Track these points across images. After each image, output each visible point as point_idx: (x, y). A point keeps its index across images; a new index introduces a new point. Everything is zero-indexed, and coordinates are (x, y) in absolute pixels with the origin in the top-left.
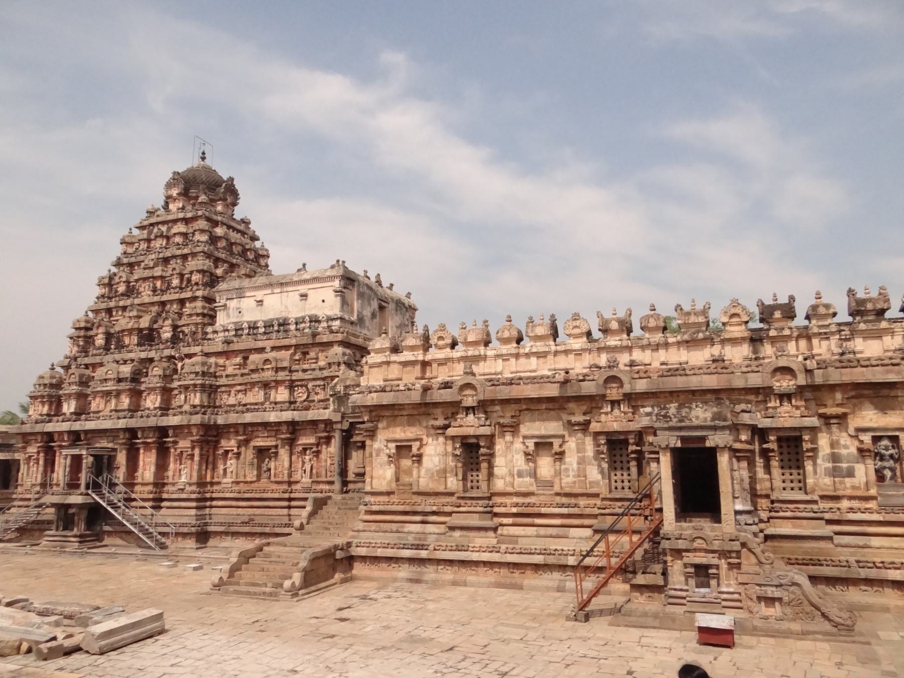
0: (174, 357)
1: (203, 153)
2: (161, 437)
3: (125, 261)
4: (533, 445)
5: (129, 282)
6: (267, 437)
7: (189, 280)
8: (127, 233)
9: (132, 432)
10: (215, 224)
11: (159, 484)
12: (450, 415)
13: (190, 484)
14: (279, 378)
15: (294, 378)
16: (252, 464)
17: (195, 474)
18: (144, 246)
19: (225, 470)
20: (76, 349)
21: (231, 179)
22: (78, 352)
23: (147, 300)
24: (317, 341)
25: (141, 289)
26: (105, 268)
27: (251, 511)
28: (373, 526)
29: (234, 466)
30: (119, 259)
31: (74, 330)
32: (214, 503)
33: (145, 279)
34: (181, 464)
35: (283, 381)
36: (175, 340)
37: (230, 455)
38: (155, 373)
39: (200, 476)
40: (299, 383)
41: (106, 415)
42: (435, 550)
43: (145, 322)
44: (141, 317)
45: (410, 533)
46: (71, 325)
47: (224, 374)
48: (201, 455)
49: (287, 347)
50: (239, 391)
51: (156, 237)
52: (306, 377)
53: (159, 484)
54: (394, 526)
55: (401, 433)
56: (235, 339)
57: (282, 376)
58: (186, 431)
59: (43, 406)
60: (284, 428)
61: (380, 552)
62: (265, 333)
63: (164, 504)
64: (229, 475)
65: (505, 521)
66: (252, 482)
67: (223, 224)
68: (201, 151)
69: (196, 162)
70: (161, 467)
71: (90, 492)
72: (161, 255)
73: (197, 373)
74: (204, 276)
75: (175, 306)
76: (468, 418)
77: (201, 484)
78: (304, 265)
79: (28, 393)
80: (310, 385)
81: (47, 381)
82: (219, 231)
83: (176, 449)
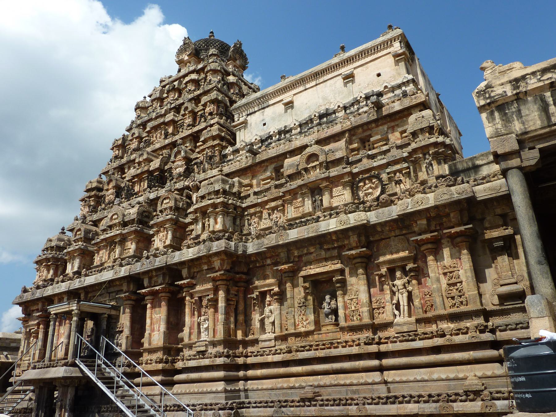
3: (139, 122)
9: (135, 280)
10: (228, 74)
11: (172, 348)
13: (214, 344)
15: (355, 171)
16: (304, 305)
17: (220, 328)
19: (262, 322)
22: (88, 212)
23: (158, 146)
24: (385, 113)
27: (312, 380)
29: (277, 312)
32: (250, 373)
34: (200, 315)
36: (188, 173)
37: (268, 298)
38: (164, 206)
39: (227, 331)
41: (110, 268)
43: (156, 164)
47: (251, 192)
48: (227, 300)
49: (335, 137)
50: (273, 209)
51: (168, 93)
52: (375, 164)
53: (172, 348)
58: (206, 267)
59: (48, 271)
63: (177, 377)
64: (268, 328)
66: (308, 334)
70: (175, 324)
71: (77, 362)
73: (217, 192)
74: (218, 107)
77: (229, 342)
80: (384, 176)
81: (53, 244)
83: (192, 296)
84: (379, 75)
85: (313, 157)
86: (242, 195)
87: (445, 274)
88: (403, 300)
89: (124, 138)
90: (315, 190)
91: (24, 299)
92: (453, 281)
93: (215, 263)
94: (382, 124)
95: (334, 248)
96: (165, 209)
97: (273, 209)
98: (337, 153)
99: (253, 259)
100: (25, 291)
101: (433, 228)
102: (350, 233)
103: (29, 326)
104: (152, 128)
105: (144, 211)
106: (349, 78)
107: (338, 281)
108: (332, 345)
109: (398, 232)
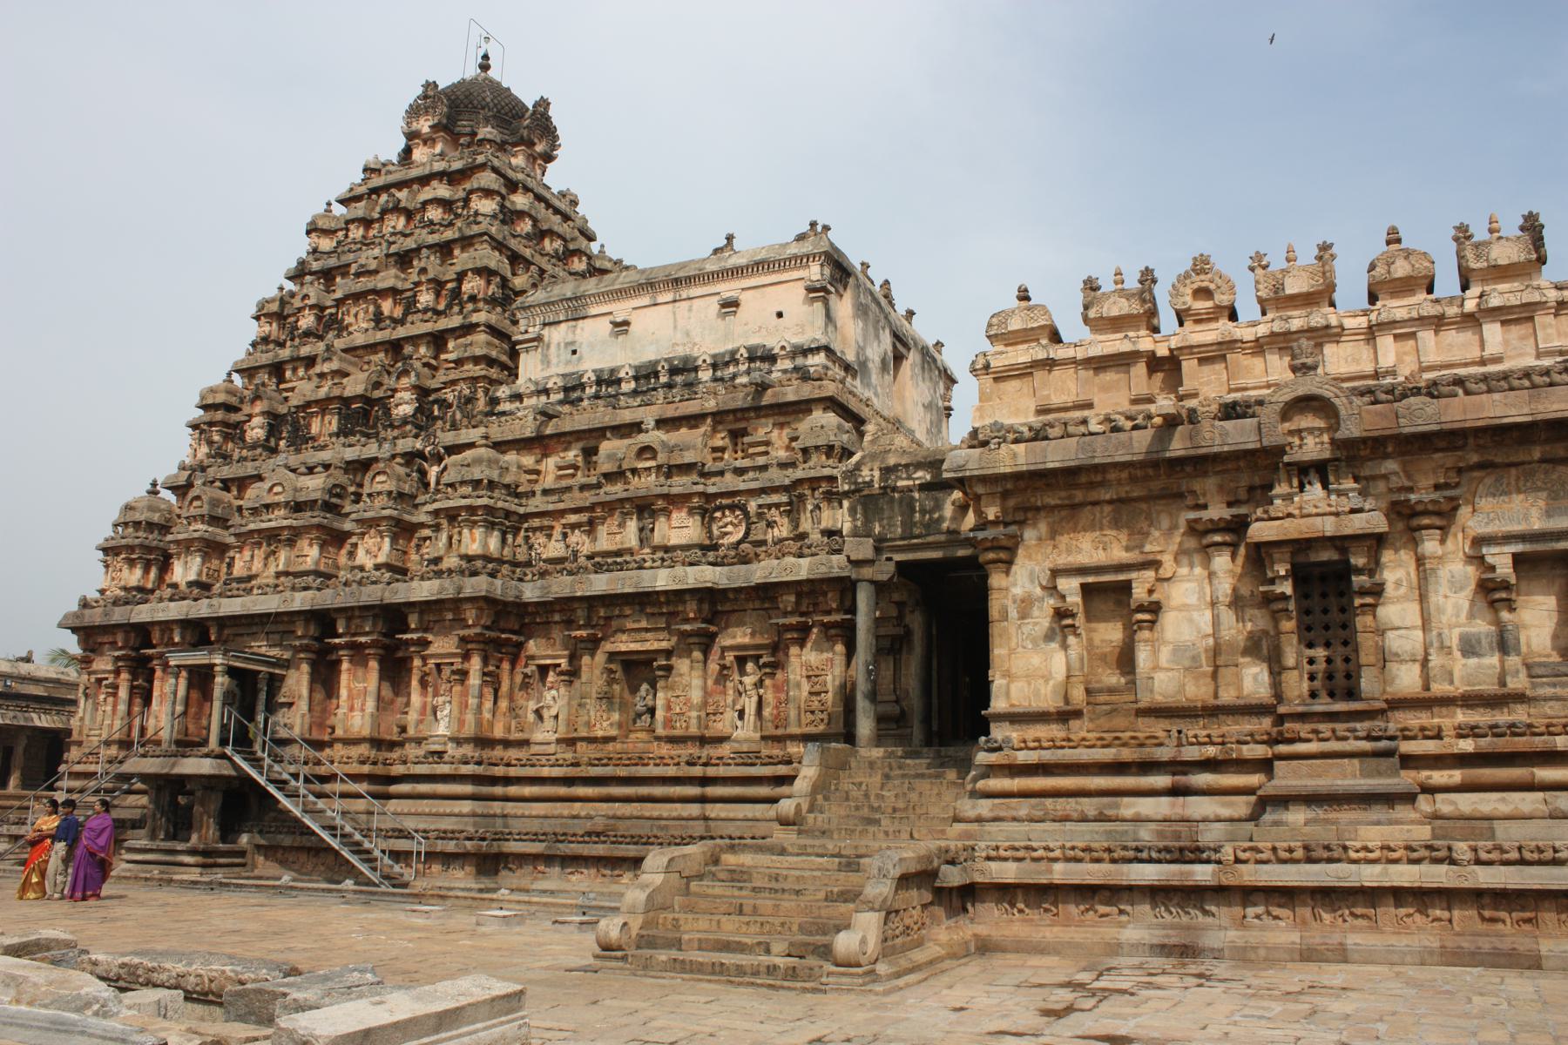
0: (420, 454)
1: (486, 57)
2: (389, 634)
3: (315, 266)
4: (1509, 560)
5: (322, 309)
6: (647, 630)
7: (456, 293)
8: (321, 209)
9: (323, 620)
10: (512, 186)
12: (1243, 495)
14: (675, 491)
15: (711, 490)
17: (470, 717)
18: (357, 233)
20: (204, 449)
21: (543, 104)
22: (209, 456)
23: (359, 339)
25: (349, 320)
26: (271, 282)
27: (604, 807)
28: (1024, 807)
29: (561, 702)
30: (302, 263)
31: (201, 412)
32: (513, 790)
33: (357, 297)
34: (436, 694)
35: (686, 497)
36: (423, 420)
37: (551, 677)
38: (379, 488)
40: (725, 502)
41: (268, 582)
42: (1238, 861)
43: (355, 385)
44: (347, 375)
45: (1138, 820)
46: (197, 400)
47: (538, 488)
49: (693, 420)
50: (574, 526)
51: (384, 212)
52: (742, 486)
54: (1089, 806)
55: (1095, 548)
56: (566, 408)
57: (680, 484)
58: (450, 616)
60: (691, 609)
61: (1060, 873)
62: (635, 393)
63: (394, 789)
65: (1439, 777)
66: (607, 740)
67: (527, 189)
68: (481, 53)
69: (471, 71)
71: (229, 750)
72: (393, 249)
73: (477, 484)
74: (489, 283)
75: (423, 350)
76: (1306, 496)
78: (730, 238)
79: (101, 541)
80: (752, 506)
81: (138, 517)
82: (520, 201)
83: (424, 659)
84: (780, 315)
85: (646, 451)
86: (520, 490)
87: (809, 677)
88: (750, 705)
89: (283, 302)
90: (645, 508)
91: (87, 622)
92: (817, 688)
93: (468, 614)
94: (766, 416)
95: (662, 614)
96: (379, 493)
97: (574, 526)
98: (686, 453)
99: (530, 609)
100: (85, 604)
101: (804, 609)
102: (687, 597)
103: (94, 672)
104: (346, 297)
105: (335, 486)
106: (730, 305)
107: (660, 668)
108: (641, 761)
109: (757, 604)
